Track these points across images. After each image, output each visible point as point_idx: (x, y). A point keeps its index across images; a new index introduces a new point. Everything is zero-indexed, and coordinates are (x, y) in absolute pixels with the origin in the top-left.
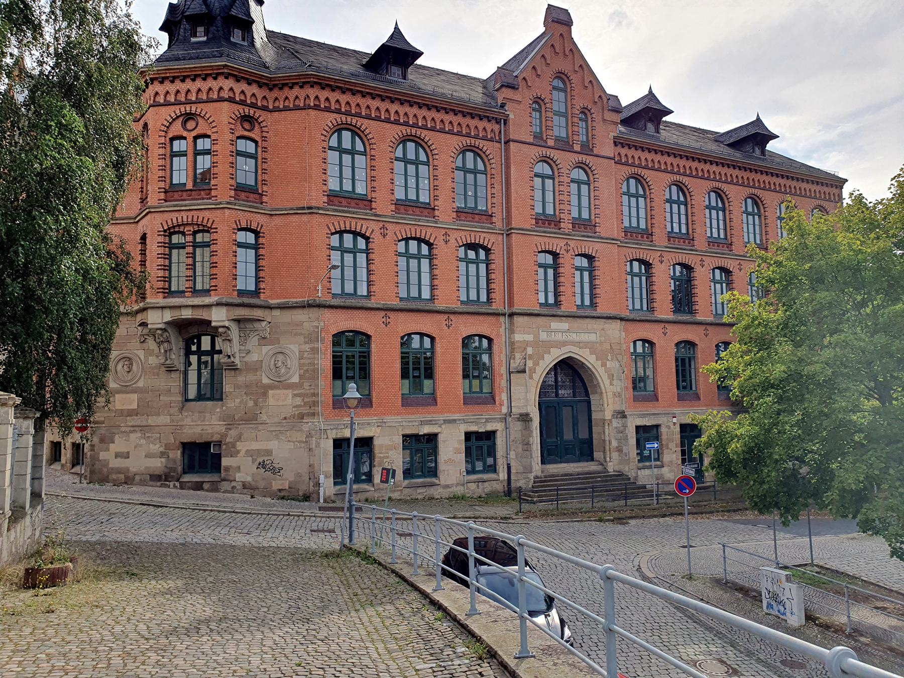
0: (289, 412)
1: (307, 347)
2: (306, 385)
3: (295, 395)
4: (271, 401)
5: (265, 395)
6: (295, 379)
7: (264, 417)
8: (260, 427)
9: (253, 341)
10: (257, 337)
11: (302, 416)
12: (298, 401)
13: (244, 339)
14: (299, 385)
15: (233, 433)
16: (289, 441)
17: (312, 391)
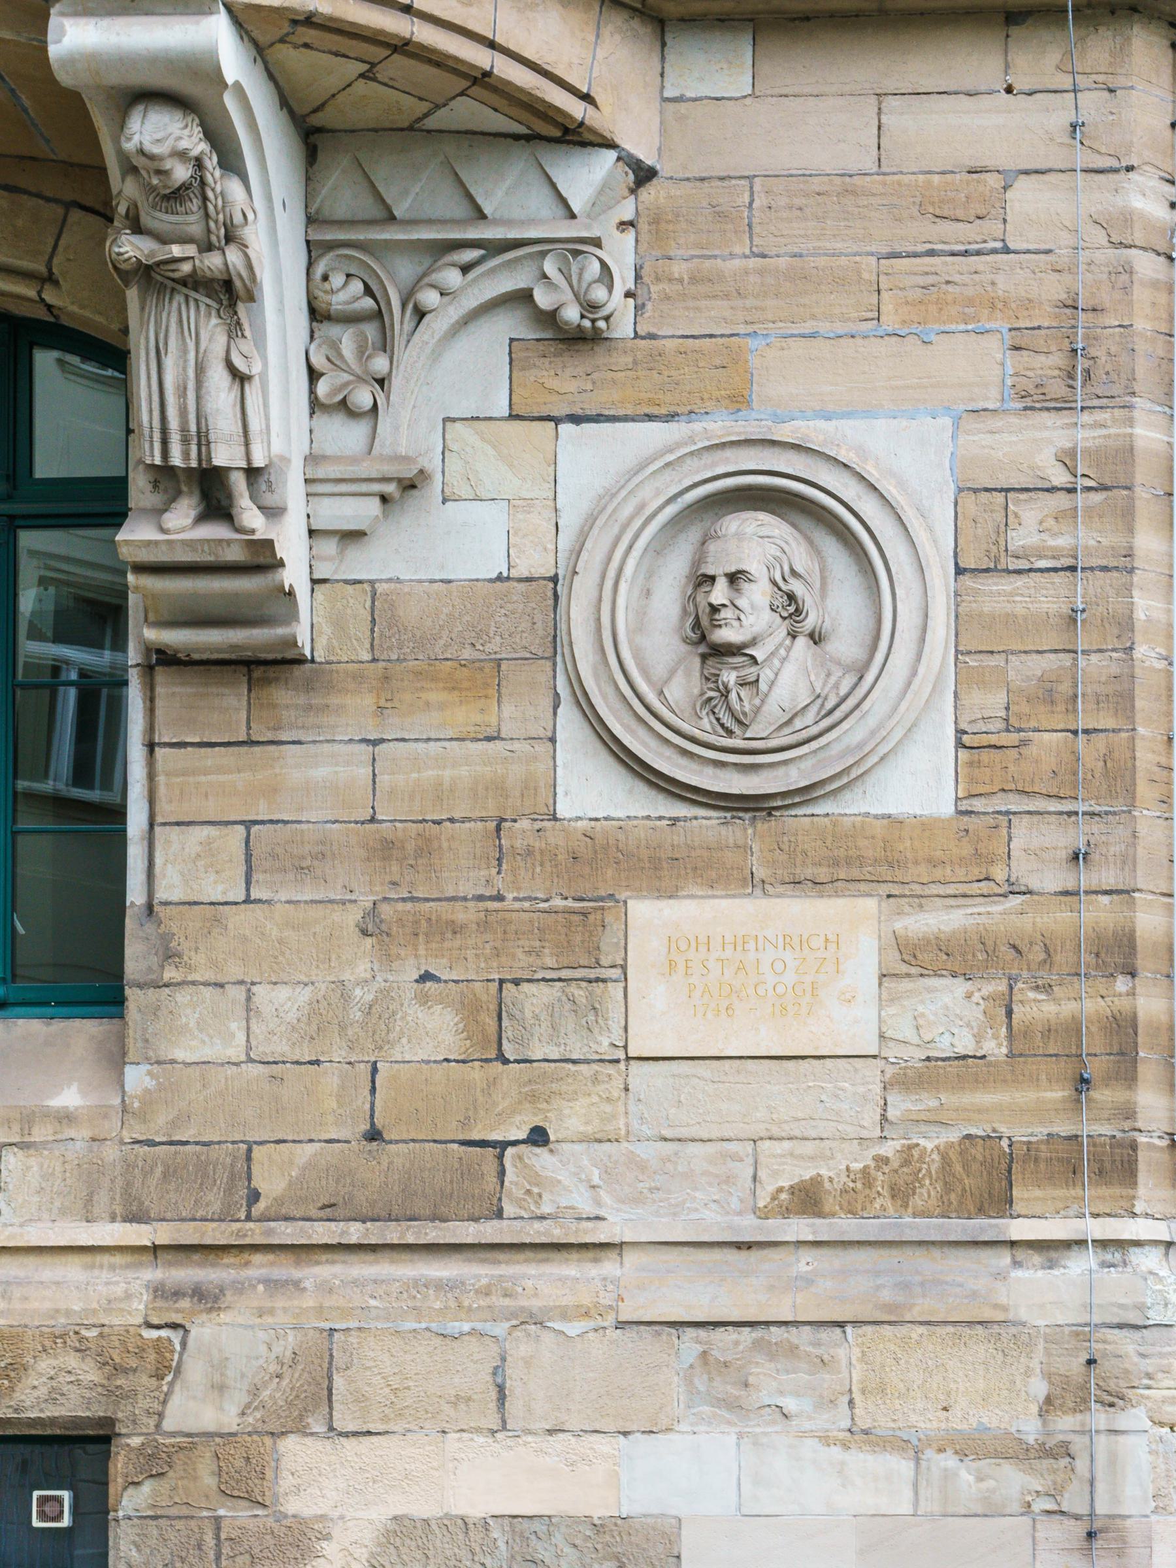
0: (840, 1127)
1: (1037, 445)
2: (1036, 849)
3: (915, 960)
4: (657, 1012)
6: (917, 784)
7: (564, 1185)
8: (543, 1282)
9: (455, 370)
10: (508, 326)
11: (990, 1180)
12: (951, 1016)
13: (361, 322)
14: (970, 850)
15: (235, 1348)
16: (862, 1436)
17: (1100, 914)
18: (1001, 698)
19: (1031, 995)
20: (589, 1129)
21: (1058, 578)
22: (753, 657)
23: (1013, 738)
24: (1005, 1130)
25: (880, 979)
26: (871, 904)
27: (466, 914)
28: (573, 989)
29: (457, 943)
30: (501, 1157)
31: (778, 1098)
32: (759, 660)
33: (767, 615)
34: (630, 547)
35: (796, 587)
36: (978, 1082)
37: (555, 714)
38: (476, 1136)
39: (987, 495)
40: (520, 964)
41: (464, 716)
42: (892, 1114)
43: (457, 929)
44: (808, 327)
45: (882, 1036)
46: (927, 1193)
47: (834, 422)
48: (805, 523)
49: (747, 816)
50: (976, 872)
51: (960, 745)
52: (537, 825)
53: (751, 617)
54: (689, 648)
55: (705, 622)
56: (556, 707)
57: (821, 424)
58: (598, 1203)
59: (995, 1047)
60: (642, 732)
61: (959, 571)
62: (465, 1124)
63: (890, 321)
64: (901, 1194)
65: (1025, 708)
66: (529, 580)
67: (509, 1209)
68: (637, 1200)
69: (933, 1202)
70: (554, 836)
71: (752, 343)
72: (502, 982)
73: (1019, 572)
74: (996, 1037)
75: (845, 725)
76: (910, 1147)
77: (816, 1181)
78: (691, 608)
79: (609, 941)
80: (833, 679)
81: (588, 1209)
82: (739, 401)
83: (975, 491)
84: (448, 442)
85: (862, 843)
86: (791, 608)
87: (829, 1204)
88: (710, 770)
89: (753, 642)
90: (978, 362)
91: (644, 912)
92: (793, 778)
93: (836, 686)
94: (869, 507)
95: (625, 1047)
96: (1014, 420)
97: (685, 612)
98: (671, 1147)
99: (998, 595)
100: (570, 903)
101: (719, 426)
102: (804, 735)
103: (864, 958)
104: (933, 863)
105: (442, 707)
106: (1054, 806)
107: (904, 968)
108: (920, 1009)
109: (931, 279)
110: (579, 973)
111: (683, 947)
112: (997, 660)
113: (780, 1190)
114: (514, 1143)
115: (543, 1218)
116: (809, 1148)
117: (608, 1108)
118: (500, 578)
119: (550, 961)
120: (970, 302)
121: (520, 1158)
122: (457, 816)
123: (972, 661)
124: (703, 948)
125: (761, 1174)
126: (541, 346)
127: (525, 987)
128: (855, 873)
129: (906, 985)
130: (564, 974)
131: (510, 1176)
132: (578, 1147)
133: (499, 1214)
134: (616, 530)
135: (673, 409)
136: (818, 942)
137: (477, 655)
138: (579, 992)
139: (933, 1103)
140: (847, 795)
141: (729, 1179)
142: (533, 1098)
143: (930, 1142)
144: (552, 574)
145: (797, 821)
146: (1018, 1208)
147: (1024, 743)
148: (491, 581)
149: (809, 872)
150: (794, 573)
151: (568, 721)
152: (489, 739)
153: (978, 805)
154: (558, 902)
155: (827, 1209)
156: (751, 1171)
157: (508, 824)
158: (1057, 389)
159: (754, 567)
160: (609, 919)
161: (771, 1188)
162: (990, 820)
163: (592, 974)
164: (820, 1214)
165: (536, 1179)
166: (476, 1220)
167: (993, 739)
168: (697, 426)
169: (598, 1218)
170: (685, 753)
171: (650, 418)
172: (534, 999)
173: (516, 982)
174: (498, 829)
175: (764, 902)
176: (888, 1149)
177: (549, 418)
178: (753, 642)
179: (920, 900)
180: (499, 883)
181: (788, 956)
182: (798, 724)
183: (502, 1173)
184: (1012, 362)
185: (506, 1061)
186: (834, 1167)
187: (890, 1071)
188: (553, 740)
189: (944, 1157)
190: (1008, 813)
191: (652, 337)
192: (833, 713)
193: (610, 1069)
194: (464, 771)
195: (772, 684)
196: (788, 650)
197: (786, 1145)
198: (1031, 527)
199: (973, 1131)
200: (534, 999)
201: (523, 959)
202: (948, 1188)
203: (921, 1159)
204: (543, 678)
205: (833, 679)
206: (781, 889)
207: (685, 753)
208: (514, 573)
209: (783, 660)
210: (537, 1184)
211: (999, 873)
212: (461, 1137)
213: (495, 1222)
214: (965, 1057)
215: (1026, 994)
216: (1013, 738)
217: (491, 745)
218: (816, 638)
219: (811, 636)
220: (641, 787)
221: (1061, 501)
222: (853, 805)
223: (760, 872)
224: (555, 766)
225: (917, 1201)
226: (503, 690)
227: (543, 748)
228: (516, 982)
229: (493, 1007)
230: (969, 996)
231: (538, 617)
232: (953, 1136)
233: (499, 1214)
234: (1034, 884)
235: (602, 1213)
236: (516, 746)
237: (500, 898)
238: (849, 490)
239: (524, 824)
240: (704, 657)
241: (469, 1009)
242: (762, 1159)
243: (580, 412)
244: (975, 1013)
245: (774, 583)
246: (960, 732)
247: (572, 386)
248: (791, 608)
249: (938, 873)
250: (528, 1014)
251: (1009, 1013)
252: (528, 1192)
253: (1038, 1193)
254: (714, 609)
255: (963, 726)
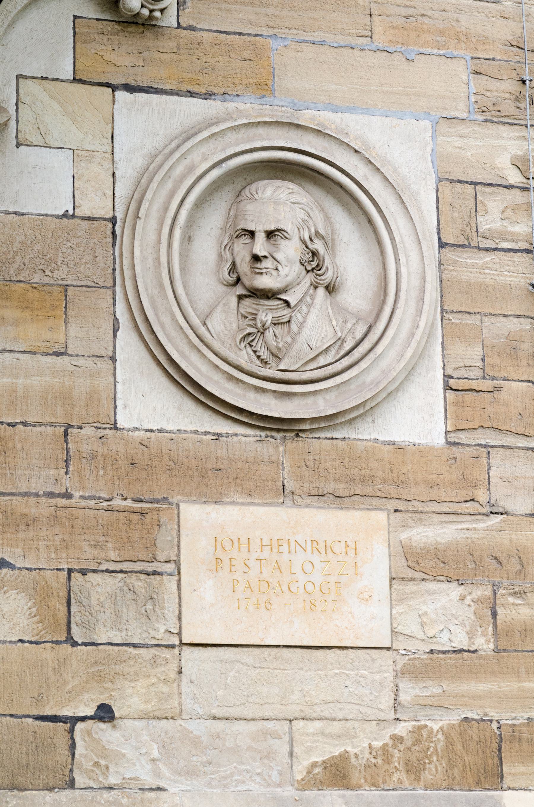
3: (418, 567)
4: (207, 605)
5: (140, 545)
6: (417, 419)
14: (455, 478)
18: (477, 351)
19: (511, 600)
20: (149, 707)
21: (518, 258)
22: (287, 303)
23: (487, 385)
24: (493, 714)
25: (391, 582)
26: (381, 517)
27: (39, 509)
28: (133, 580)
29: (30, 534)
30: (71, 731)
31: (312, 683)
32: (293, 303)
33: (297, 267)
34: (182, 201)
35: (318, 246)
36: (473, 673)
37: (115, 336)
38: (49, 712)
39: (461, 185)
40: (87, 556)
41: (34, 333)
42: (404, 698)
43: (29, 522)
44: (317, 36)
45: (393, 631)
46: (434, 769)
47: (340, 115)
48: (319, 193)
49: (279, 435)
50: (464, 494)
51: (448, 387)
52: (101, 433)
53: (284, 269)
54: (225, 289)
55: (244, 267)
56: (115, 331)
57: (330, 115)
58: (158, 775)
59: (484, 643)
60: (194, 357)
61: (442, 245)
62: (38, 700)
63: (380, 40)
64: (414, 769)
65: (495, 360)
66: (90, 219)
67: (80, 780)
68: (191, 773)
69: (440, 776)
70: (114, 443)
71: (274, 44)
72: (70, 571)
73: (487, 250)
74: (484, 634)
75: (363, 365)
76: (420, 728)
77: (344, 757)
78: (228, 255)
79: (164, 538)
80: (349, 325)
81: (151, 781)
82: (264, 89)
83: (451, 181)
84: (21, 96)
85: (373, 464)
86: (313, 263)
87: (355, 778)
88: (252, 395)
89: (285, 290)
90: (450, 81)
91: (194, 514)
92: (322, 407)
93: (352, 331)
94: (374, 185)
95: (179, 634)
96: (477, 129)
97: (221, 257)
98: (220, 725)
99: (471, 266)
100: (129, 503)
101: (248, 108)
102: (331, 370)
103: (377, 565)
104: (432, 485)
105: (16, 323)
106: (522, 443)
107: (411, 573)
108: (424, 608)
109: (410, 11)
110: (139, 566)
111: (228, 546)
112: (474, 320)
113: (314, 765)
114: (84, 719)
115: (110, 788)
116: (336, 727)
117: (165, 689)
118: (65, 215)
119: (113, 555)
120: (441, 33)
121: (89, 733)
122: (29, 420)
123: (455, 319)
124: (244, 549)
125: (297, 750)
126: (100, 25)
127: (91, 576)
128: (369, 490)
129: (411, 587)
130: (125, 566)
131: (80, 750)
132: (139, 724)
133: (71, 784)
134: (169, 185)
135: (210, 89)
136: (339, 548)
137: (47, 280)
138: (139, 583)
139: (438, 690)
140: (360, 424)
141: (269, 755)
142: (99, 678)
143: (437, 723)
144: (110, 215)
145: (317, 444)
146: (507, 781)
147: (498, 389)
148: (58, 217)
149: (331, 487)
150: (317, 234)
151: (127, 344)
152: (58, 354)
153: (463, 438)
154: (118, 502)
155: (354, 781)
156: (286, 748)
157: (77, 429)
158: (509, 108)
159: (288, 227)
160: (164, 519)
161: (306, 763)
162: (473, 451)
163: (150, 567)
164: (348, 787)
165: (104, 752)
166: (50, 789)
167: (473, 384)
168: (231, 106)
169: (159, 789)
170: (231, 378)
171: (191, 94)
172: (99, 588)
173: (83, 572)
174: (66, 434)
175: (294, 511)
176: (402, 729)
177: (107, 85)
178: (285, 290)
179: (420, 516)
180: (67, 483)
181: (316, 558)
182: (322, 361)
183: (73, 746)
184: (475, 83)
185: (75, 644)
186: (361, 745)
187: (401, 662)
188: (113, 359)
189: (447, 737)
190: (486, 446)
191: (192, 28)
192: (351, 353)
193: (166, 653)
194: (35, 381)
195: (301, 326)
196: (313, 297)
197: (318, 724)
198: (495, 215)
199: (469, 715)
200: (99, 588)
201: (89, 553)
202: (451, 764)
203: (429, 739)
204: (105, 304)
205: (349, 325)
206: (308, 500)
207: (231, 378)
208: (78, 212)
209: (310, 306)
210: (105, 757)
211: (482, 496)
212: (35, 712)
213: (68, 792)
214: (461, 651)
215: (506, 599)
216: (487, 385)
217: (59, 359)
218: (330, 289)
219: (327, 288)
220: (189, 404)
221: (516, 196)
222: (367, 432)
223: (290, 486)
224: (115, 382)
225: (427, 776)
226: (70, 313)
227: (105, 365)
228: (83, 572)
229: (63, 594)
230: (462, 599)
231: (100, 252)
232: (454, 718)
233: (71, 784)
234: (509, 506)
235: (162, 785)
236: (81, 362)
237: (68, 496)
238: (359, 170)
239: (88, 431)
240: (240, 297)
241: (40, 595)
242: (297, 737)
243: (133, 83)
244: (467, 613)
245: (304, 242)
246: (447, 377)
247: (127, 61)
248: (313, 263)
249: (435, 493)
250: (94, 602)
251: (494, 614)
252: (96, 764)
253: (522, 769)
254: (256, 258)
255: (449, 372)
